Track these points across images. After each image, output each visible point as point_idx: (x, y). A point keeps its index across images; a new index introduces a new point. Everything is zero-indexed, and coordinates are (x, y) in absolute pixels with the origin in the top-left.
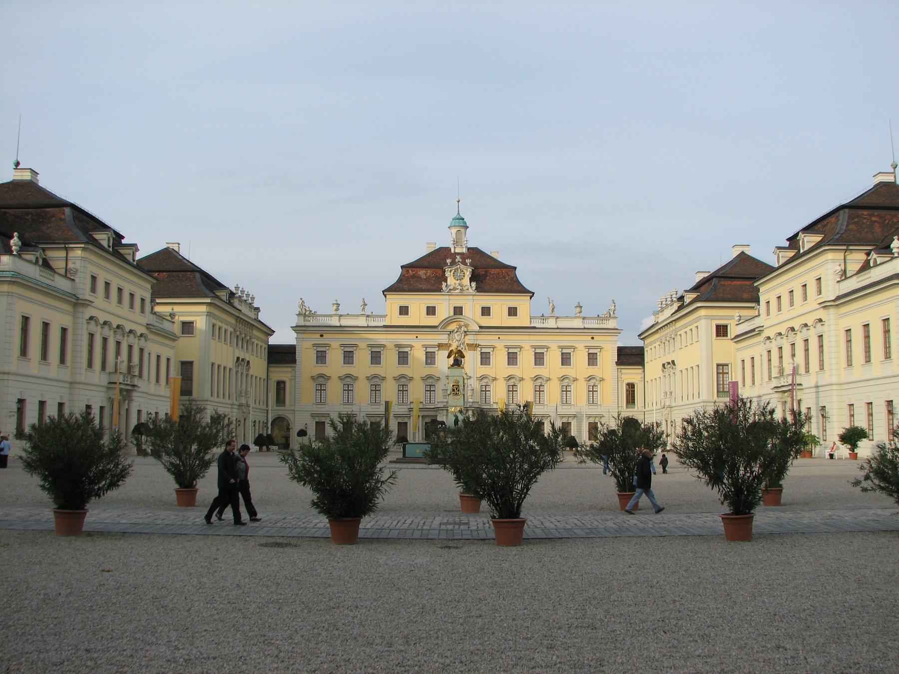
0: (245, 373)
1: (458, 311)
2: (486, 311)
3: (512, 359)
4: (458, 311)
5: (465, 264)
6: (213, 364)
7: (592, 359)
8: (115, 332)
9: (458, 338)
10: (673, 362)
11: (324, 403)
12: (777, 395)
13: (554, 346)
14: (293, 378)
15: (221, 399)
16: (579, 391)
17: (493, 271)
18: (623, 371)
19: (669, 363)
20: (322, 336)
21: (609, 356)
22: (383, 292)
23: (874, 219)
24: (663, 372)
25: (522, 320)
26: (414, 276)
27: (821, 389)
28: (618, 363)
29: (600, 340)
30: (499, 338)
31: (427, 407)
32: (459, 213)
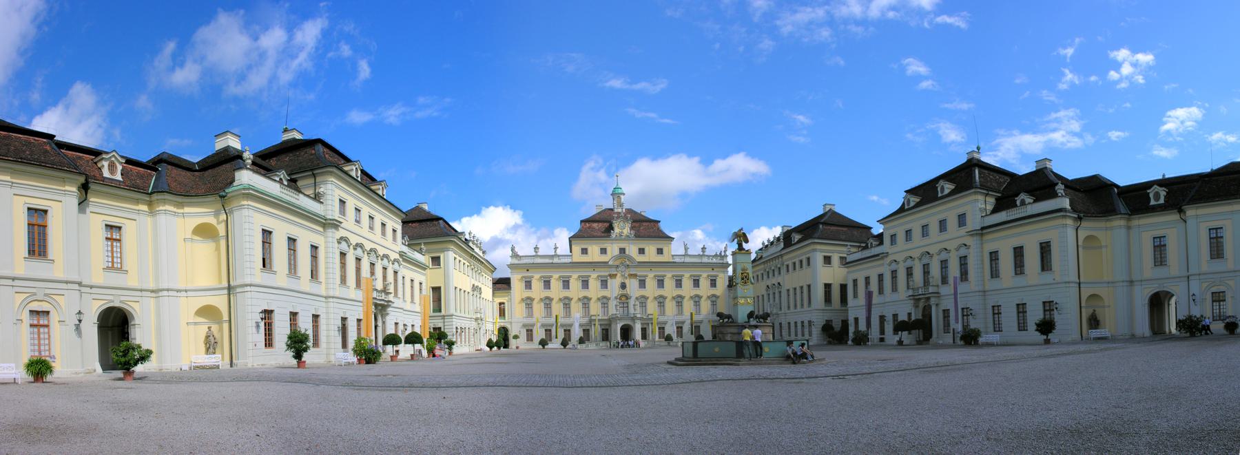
0: (478, 296)
1: (622, 251)
2: (642, 251)
4: (622, 251)
6: (456, 288)
7: (713, 283)
8: (368, 253)
10: (779, 283)
12: (912, 302)
15: (463, 315)
17: (644, 224)
19: (774, 285)
24: (767, 291)
26: (589, 228)
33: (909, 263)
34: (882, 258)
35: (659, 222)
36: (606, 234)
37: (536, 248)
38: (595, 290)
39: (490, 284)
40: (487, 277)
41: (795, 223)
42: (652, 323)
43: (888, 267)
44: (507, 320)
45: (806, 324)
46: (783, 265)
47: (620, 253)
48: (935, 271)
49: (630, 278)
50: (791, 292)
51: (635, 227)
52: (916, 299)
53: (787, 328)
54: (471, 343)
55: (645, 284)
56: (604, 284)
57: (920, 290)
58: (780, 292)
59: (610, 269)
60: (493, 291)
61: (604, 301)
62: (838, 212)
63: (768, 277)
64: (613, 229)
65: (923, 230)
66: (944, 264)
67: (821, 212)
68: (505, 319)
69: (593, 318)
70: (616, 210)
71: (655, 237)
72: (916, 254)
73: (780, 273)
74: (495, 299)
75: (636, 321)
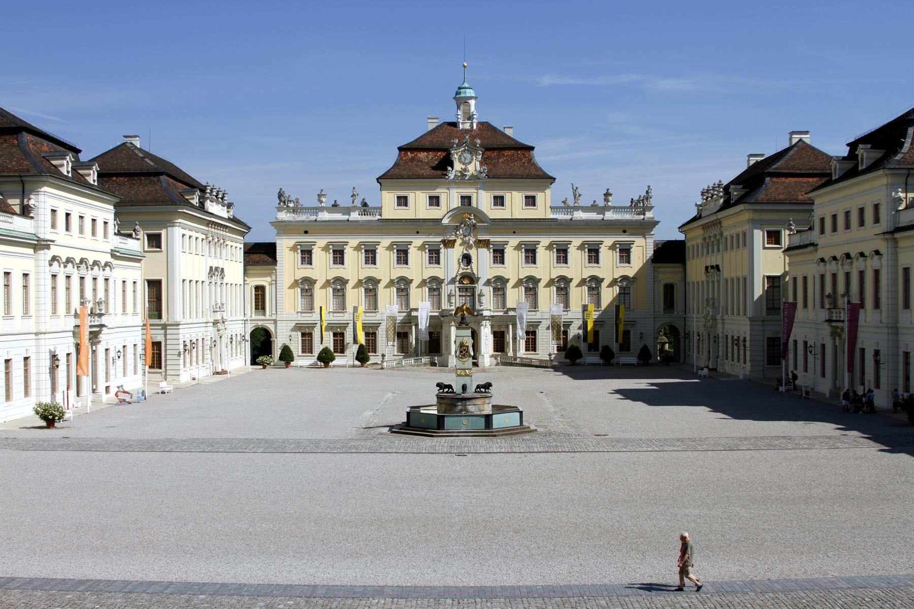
1: (466, 200)
4: (466, 200)
14: (274, 282)
17: (506, 153)
18: (660, 270)
22: (377, 179)
25: (541, 211)
26: (413, 159)
35: (532, 148)
36: (439, 172)
39: (240, 255)
40: (234, 244)
44: (267, 317)
49: (478, 247)
51: (489, 158)
54: (205, 361)
56: (435, 256)
60: (245, 266)
64: (451, 164)
68: (264, 314)
69: (414, 314)
71: (522, 177)
74: (249, 280)
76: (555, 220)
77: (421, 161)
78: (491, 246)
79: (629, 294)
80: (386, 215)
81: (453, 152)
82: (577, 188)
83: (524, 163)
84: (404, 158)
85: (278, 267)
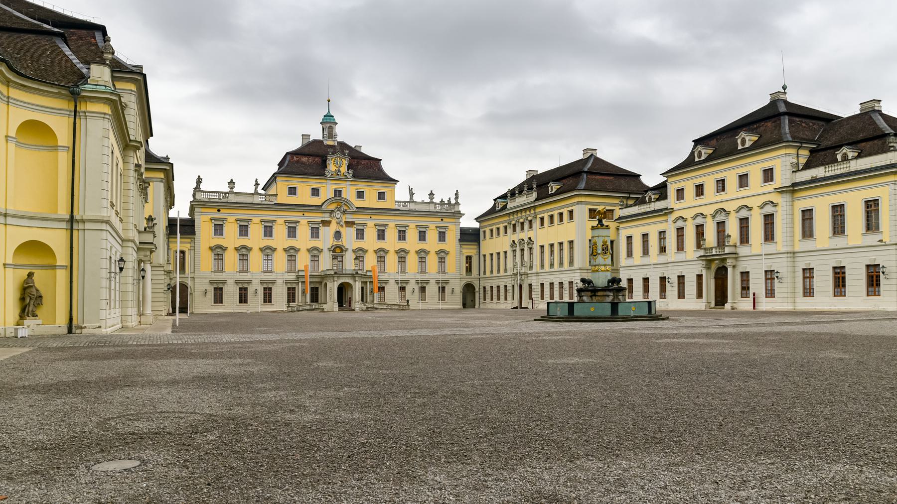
1: (338, 193)
2: (360, 195)
3: (381, 235)
4: (338, 193)
5: (344, 154)
7: (442, 236)
9: (338, 217)
11: (222, 271)
12: (704, 263)
13: (412, 225)
16: (432, 262)
17: (363, 162)
19: (523, 240)
20: (219, 211)
21: (453, 236)
23: (803, 125)
24: (512, 246)
26: (298, 162)
27: (797, 255)
28: (460, 240)
29: (447, 222)
30: (371, 217)
31: (312, 274)
32: (329, 111)
33: (699, 220)
34: (666, 214)
35: (381, 160)
37: (231, 183)
38: (303, 239)
41: (543, 167)
42: (371, 282)
43: (673, 225)
45: (566, 285)
46: (536, 218)
47: (335, 196)
48: (733, 229)
50: (547, 250)
52: (708, 261)
53: (539, 290)
55: (363, 234)
56: (315, 233)
57: (714, 250)
58: (531, 249)
59: (324, 215)
61: (315, 253)
62: (601, 158)
63: (514, 230)
65: (717, 184)
66: (744, 223)
67: (580, 156)
69: (301, 273)
70: (327, 143)
72: (709, 211)
73: (531, 227)
75: (357, 278)
76: (398, 210)
77: (304, 164)
78: (355, 226)
79: (444, 262)
80: (280, 200)
81: (329, 158)
82: (412, 189)
83: (375, 170)
84: (291, 161)
85: (197, 237)
